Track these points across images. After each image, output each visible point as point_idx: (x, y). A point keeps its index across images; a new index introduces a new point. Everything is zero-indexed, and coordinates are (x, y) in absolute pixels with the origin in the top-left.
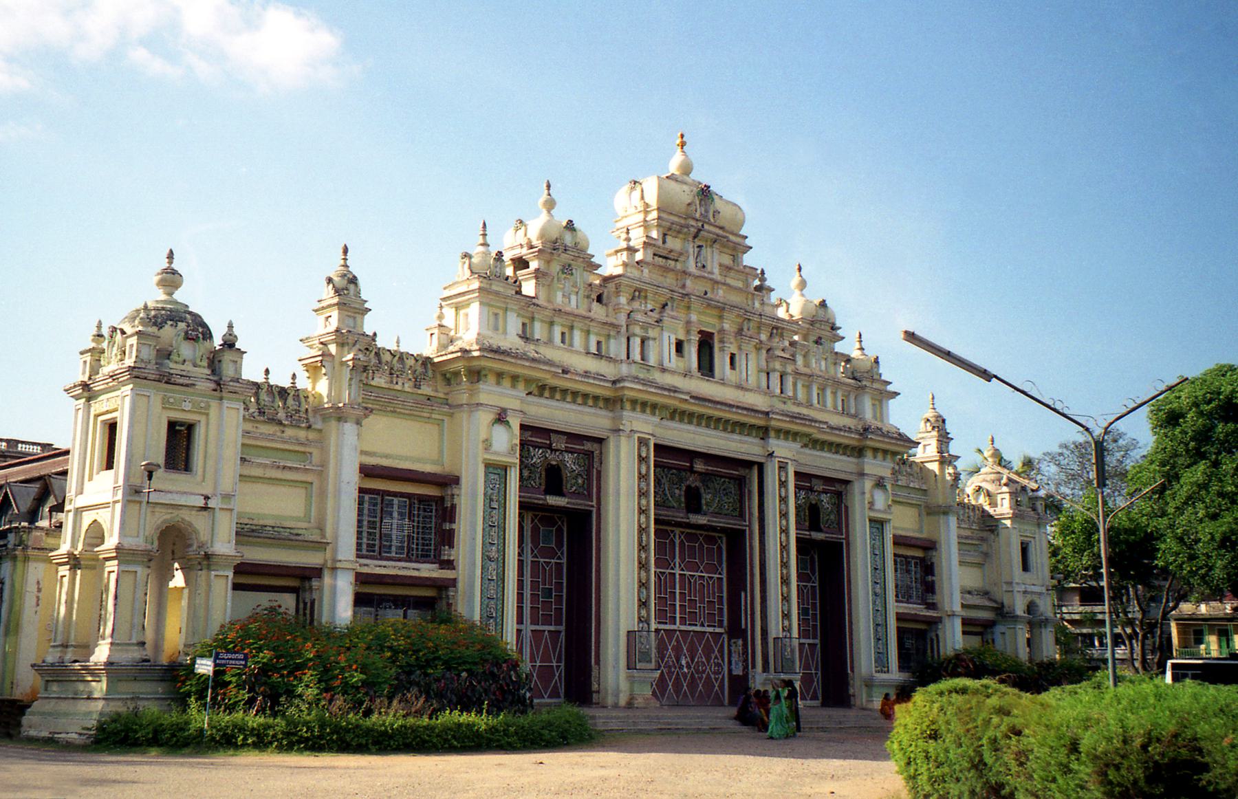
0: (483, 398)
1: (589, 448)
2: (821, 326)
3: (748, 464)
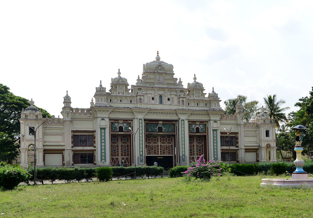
0: (99, 116)
1: (129, 122)
2: (197, 88)
3: (176, 121)
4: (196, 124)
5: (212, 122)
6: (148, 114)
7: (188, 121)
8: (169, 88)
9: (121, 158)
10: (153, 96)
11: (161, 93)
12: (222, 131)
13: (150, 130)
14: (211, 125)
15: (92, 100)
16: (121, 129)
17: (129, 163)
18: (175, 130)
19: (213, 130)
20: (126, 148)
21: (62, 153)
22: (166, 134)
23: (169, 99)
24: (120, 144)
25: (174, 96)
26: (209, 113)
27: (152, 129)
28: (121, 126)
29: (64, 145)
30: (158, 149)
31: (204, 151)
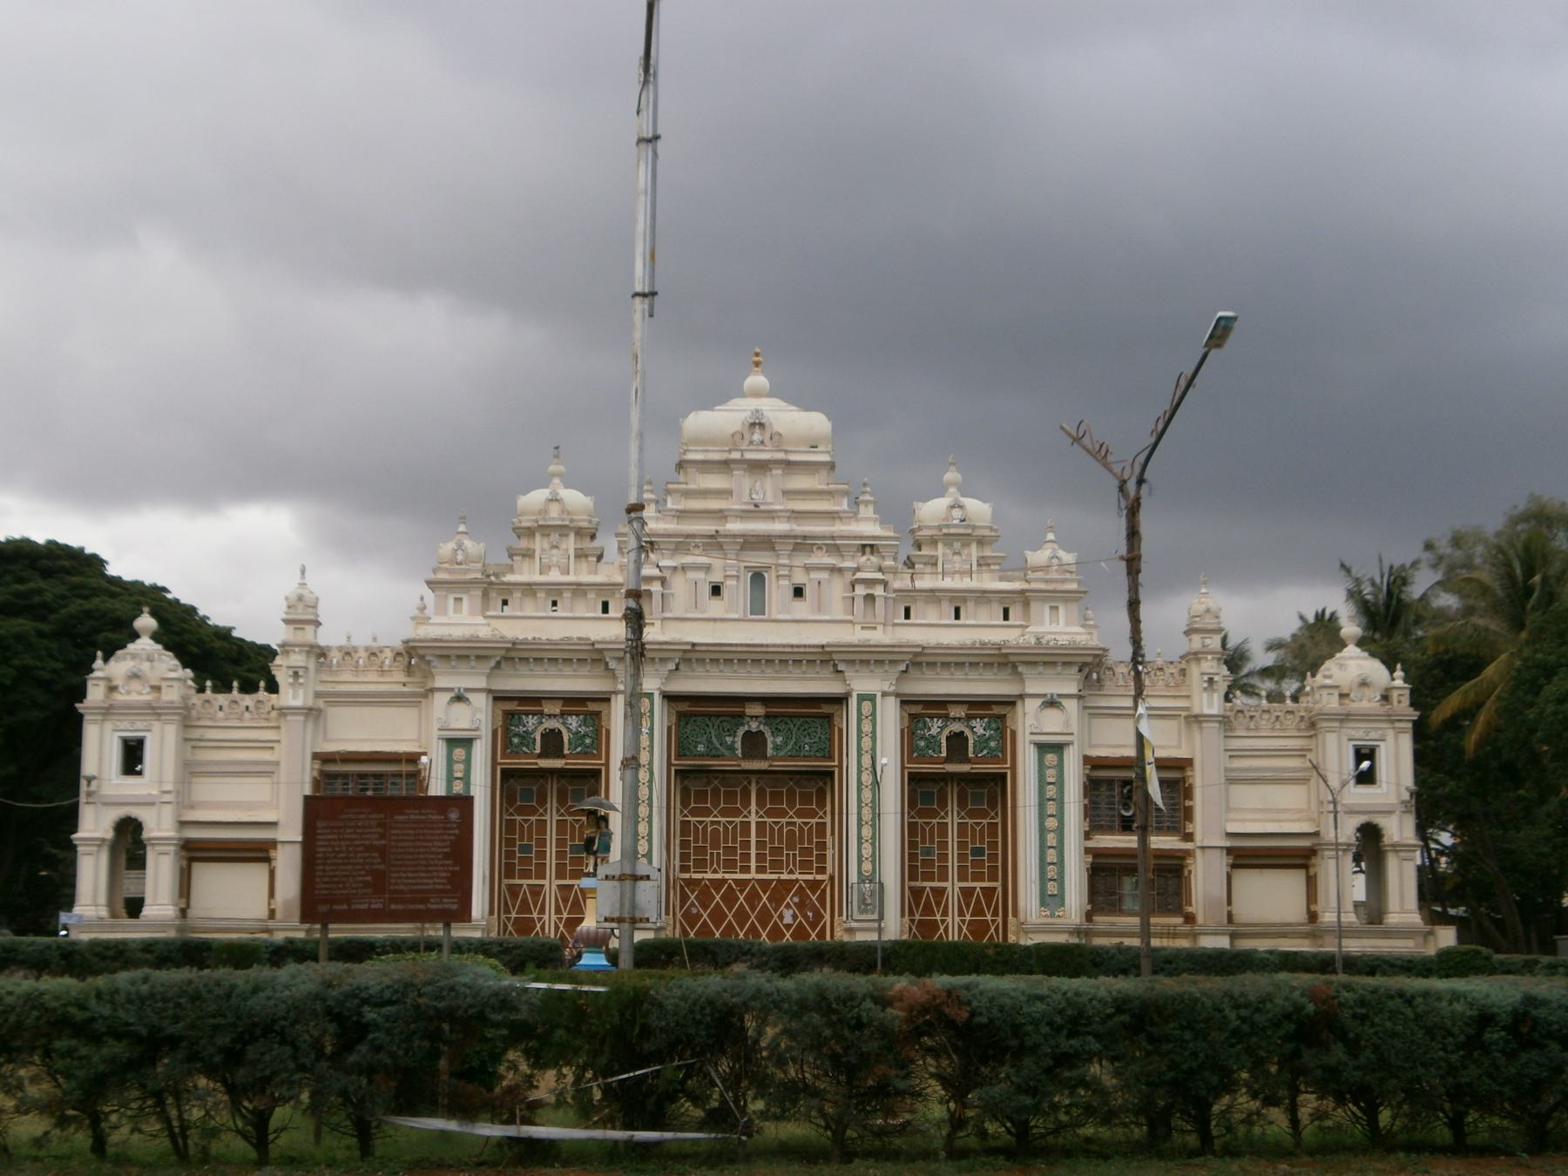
0: (440, 682)
4: (946, 717)
5: (1031, 706)
6: (913, 672)
7: (903, 703)
8: (795, 537)
9: (554, 887)
10: (716, 577)
11: (759, 559)
12: (1095, 753)
13: (701, 748)
14: (1030, 720)
15: (423, 609)
16: (552, 743)
17: (995, 913)
18: (832, 746)
19: (1043, 748)
20: (982, 842)
21: (268, 860)
22: (779, 765)
23: (798, 592)
24: (953, 819)
25: (824, 575)
26: (1012, 659)
27: (710, 742)
28: (552, 731)
29: (273, 824)
30: (746, 845)
31: (992, 857)
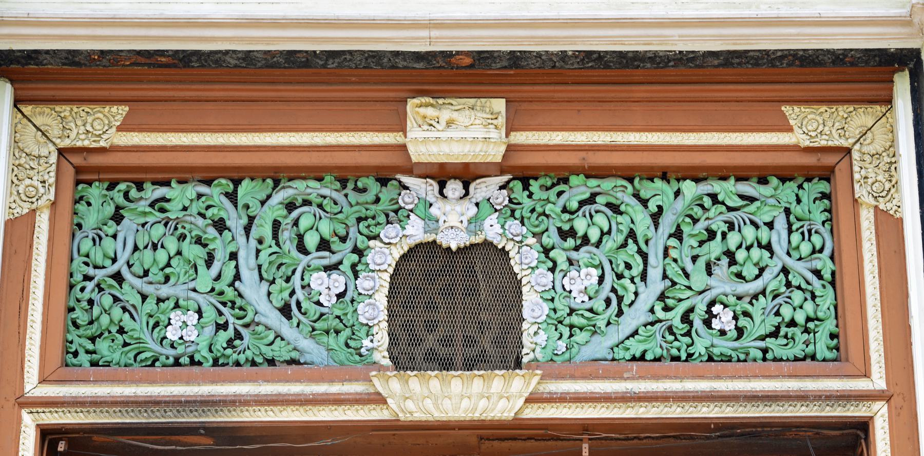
13: (184, 328)
